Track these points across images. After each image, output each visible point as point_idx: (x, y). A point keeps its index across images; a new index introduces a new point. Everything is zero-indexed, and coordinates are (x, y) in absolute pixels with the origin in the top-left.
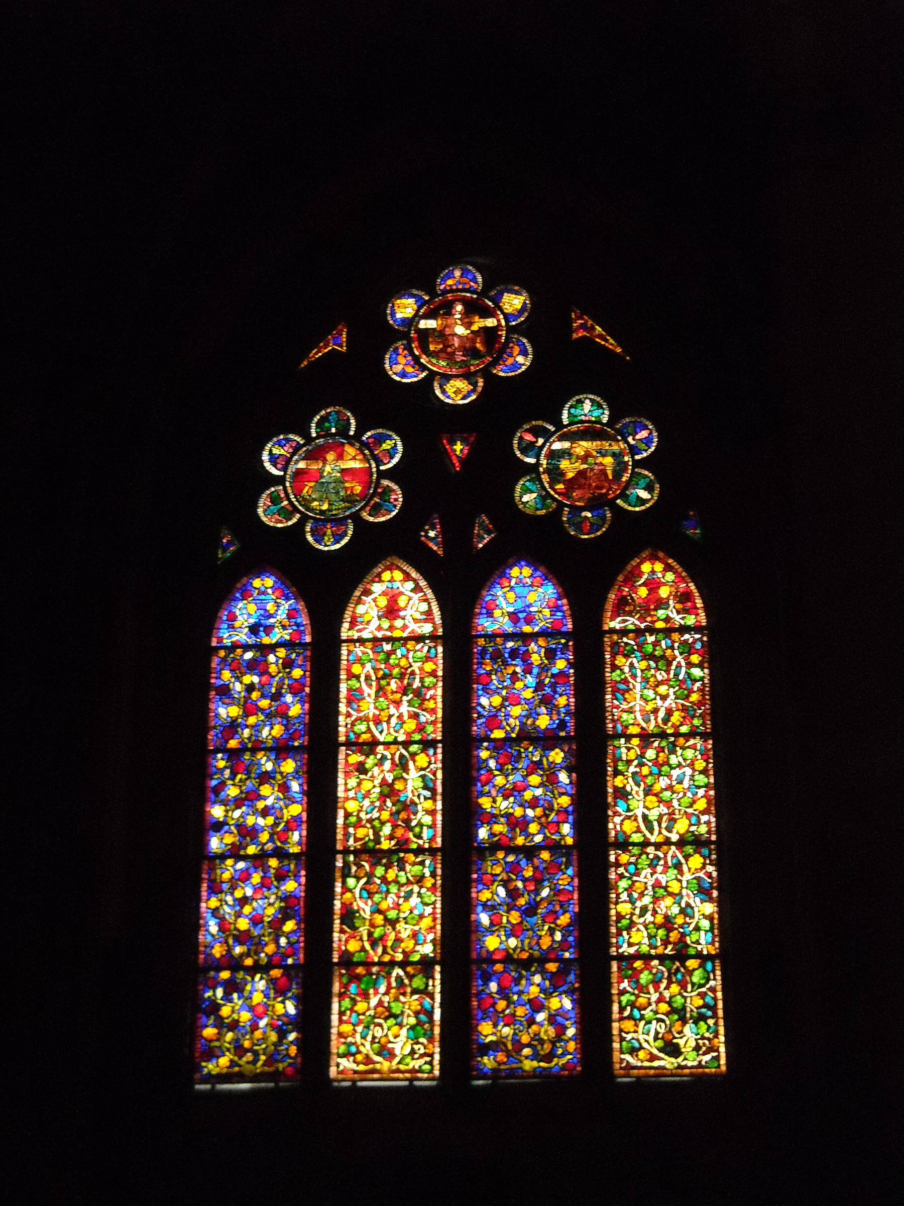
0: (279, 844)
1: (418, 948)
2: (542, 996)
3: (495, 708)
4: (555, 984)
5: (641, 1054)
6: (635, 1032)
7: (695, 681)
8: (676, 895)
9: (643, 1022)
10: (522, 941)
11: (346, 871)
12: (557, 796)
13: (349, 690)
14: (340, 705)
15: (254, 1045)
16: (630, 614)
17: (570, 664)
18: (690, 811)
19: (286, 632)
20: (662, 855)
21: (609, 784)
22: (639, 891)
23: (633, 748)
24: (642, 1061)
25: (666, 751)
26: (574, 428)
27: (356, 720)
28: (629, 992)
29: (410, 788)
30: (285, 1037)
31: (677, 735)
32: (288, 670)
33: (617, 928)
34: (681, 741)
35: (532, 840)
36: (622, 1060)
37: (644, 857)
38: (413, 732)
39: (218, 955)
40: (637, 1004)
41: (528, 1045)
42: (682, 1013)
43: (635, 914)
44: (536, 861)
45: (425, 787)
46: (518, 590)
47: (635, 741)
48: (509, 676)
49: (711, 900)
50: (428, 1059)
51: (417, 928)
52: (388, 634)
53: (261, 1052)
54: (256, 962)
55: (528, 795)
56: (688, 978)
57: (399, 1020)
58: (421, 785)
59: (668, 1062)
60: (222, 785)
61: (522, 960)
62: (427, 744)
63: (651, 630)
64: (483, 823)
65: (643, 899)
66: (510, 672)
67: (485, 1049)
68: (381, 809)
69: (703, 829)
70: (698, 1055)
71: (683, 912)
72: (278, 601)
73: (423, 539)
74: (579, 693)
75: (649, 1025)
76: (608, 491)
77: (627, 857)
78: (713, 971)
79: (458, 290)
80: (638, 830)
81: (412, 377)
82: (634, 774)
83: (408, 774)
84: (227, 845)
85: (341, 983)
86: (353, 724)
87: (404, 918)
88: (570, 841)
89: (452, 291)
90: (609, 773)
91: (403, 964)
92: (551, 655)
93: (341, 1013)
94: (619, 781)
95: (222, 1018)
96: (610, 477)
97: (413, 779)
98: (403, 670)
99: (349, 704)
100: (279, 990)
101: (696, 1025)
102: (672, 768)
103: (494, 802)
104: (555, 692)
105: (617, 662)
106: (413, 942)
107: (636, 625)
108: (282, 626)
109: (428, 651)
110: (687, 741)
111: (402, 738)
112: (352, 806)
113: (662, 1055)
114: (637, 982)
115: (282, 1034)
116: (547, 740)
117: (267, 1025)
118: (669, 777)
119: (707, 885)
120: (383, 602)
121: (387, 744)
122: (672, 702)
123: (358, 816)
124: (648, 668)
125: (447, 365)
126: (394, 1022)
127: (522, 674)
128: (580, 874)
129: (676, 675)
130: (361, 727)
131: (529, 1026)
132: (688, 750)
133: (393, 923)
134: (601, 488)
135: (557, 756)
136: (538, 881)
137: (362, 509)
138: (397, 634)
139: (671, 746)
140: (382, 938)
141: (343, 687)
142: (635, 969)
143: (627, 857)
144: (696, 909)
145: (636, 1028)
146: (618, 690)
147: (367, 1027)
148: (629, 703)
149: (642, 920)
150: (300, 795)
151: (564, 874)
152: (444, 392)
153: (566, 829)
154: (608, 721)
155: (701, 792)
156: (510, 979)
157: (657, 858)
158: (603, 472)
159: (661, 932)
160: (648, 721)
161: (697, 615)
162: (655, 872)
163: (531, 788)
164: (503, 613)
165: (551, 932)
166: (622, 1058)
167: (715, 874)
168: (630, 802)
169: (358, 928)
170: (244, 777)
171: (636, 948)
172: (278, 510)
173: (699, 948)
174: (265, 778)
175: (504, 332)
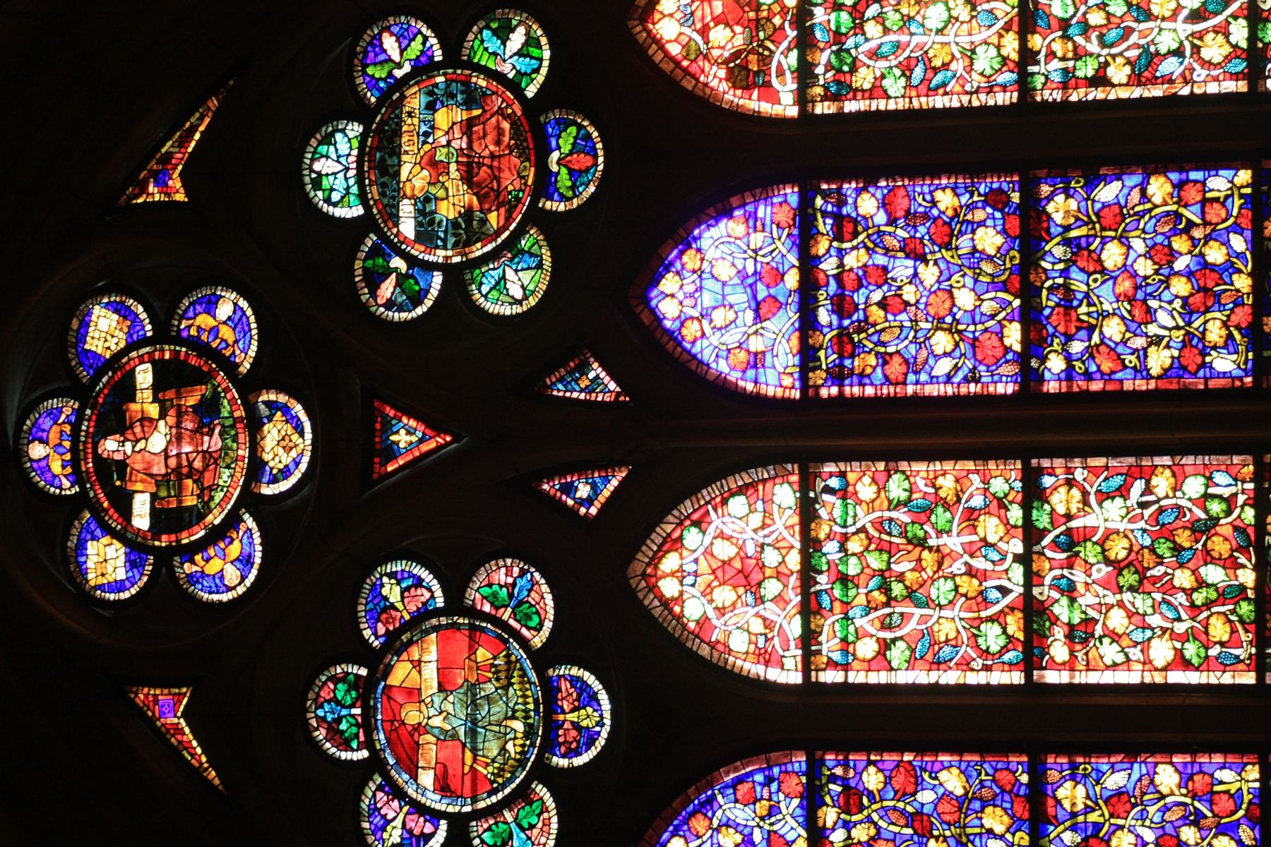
0: (1241, 813)
3: (957, 345)
12: (1148, 206)
13: (911, 663)
14: (942, 681)
16: (765, 60)
19: (782, 805)
21: (1124, 94)
23: (1049, 45)
26: (374, 192)
29: (1123, 526)
32: (865, 801)
35: (1240, 256)
45: (1123, 492)
46: (707, 300)
47: (1036, 41)
48: (890, 317)
52: (793, 581)
55: (1145, 267)
58: (1119, 501)
62: (1033, 494)
64: (1203, 365)
66: (882, 313)
68: (1170, 588)
72: (715, 823)
73: (593, 511)
74: (929, 169)
76: (506, 117)
79: (74, 450)
80: (1223, 30)
81: (251, 544)
82: (1103, 45)
83: (1095, 529)
86: (986, 653)
88: (1244, 176)
89: (75, 463)
92: (845, 227)
94: (1118, 73)
96: (480, 112)
97: (1110, 515)
98: (873, 547)
99: (937, 664)
103: (1156, 341)
104: (926, 216)
105: (867, 86)
107: (789, 49)
108: (770, 815)
111: (1017, 546)
112: (1162, 651)
120: (725, 595)
121: (1032, 578)
123: (1184, 638)
124: (880, 19)
125: (228, 467)
127: (885, 288)
130: (992, 637)
134: (500, 132)
135: (1060, 208)
137: (524, 643)
138: (794, 561)
141: (904, 678)
148: (953, 57)
150: (1136, 766)
152: (286, 473)
153: (1218, 184)
154: (991, 103)
163: (1129, 263)
164: (756, 332)
168: (1163, 51)
172: (523, 829)
175: (167, 347)
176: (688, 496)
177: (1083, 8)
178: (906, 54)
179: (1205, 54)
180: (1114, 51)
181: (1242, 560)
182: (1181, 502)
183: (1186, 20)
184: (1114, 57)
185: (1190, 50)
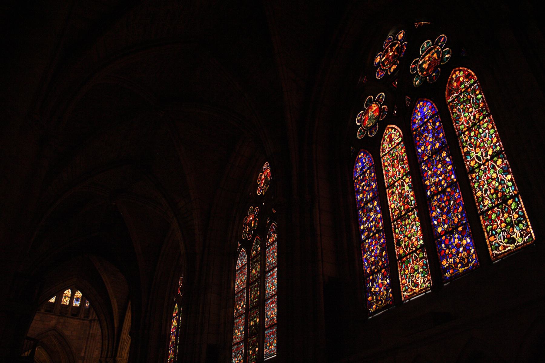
0: (377, 229)
1: (419, 243)
2: (459, 241)
4: (463, 236)
5: (500, 248)
7: (479, 100)
8: (496, 178)
9: (497, 235)
10: (449, 225)
11: (395, 228)
15: (381, 298)
16: (454, 94)
17: (440, 122)
18: (491, 145)
20: (486, 167)
22: (482, 185)
23: (467, 135)
24: (501, 251)
27: (389, 179)
28: (489, 225)
31: (479, 121)
33: (478, 203)
34: (481, 122)
35: (444, 187)
36: (493, 254)
37: (481, 171)
38: (403, 173)
39: (368, 272)
40: (493, 228)
42: (511, 224)
43: (483, 194)
44: (447, 193)
47: (467, 133)
49: (509, 173)
50: (428, 282)
53: (383, 299)
54: (378, 270)
56: (510, 208)
57: (418, 271)
59: (511, 247)
60: (362, 218)
61: (450, 231)
63: (461, 94)
67: (446, 270)
69: (498, 148)
70: (523, 239)
71: (500, 184)
75: (500, 235)
78: (519, 200)
82: (469, 144)
83: (404, 187)
87: (413, 235)
90: (461, 149)
91: (416, 250)
93: (402, 276)
95: (372, 292)
99: (386, 174)
100: (384, 276)
101: (518, 226)
102: (481, 134)
106: (417, 242)
109: (402, 146)
110: (483, 122)
112: (392, 206)
113: (508, 245)
114: (491, 220)
115: (387, 290)
116: (438, 152)
118: (481, 137)
122: (474, 112)
124: (464, 106)
126: (416, 273)
128: (461, 190)
129: (473, 102)
131: (458, 255)
132: (485, 124)
133: (410, 238)
136: (449, 200)
138: (394, 146)
139: (478, 126)
140: (408, 245)
142: (489, 215)
143: (475, 174)
144: (505, 180)
145: (495, 238)
146: (457, 120)
147: (409, 278)
149: (486, 195)
151: (456, 193)
153: (453, 176)
155: (493, 136)
157: (485, 168)
158: (435, 58)
159: (494, 196)
162: (486, 175)
165: (457, 216)
167: (508, 162)
169: (401, 245)
170: (366, 213)
171: (487, 207)
173: (511, 194)
174: (371, 210)
177: (473, 137)
178: (460, 114)
179: (471, 162)
181: (405, 211)
182: (410, 198)
183: (476, 156)
184: (468, 147)
185: (472, 159)
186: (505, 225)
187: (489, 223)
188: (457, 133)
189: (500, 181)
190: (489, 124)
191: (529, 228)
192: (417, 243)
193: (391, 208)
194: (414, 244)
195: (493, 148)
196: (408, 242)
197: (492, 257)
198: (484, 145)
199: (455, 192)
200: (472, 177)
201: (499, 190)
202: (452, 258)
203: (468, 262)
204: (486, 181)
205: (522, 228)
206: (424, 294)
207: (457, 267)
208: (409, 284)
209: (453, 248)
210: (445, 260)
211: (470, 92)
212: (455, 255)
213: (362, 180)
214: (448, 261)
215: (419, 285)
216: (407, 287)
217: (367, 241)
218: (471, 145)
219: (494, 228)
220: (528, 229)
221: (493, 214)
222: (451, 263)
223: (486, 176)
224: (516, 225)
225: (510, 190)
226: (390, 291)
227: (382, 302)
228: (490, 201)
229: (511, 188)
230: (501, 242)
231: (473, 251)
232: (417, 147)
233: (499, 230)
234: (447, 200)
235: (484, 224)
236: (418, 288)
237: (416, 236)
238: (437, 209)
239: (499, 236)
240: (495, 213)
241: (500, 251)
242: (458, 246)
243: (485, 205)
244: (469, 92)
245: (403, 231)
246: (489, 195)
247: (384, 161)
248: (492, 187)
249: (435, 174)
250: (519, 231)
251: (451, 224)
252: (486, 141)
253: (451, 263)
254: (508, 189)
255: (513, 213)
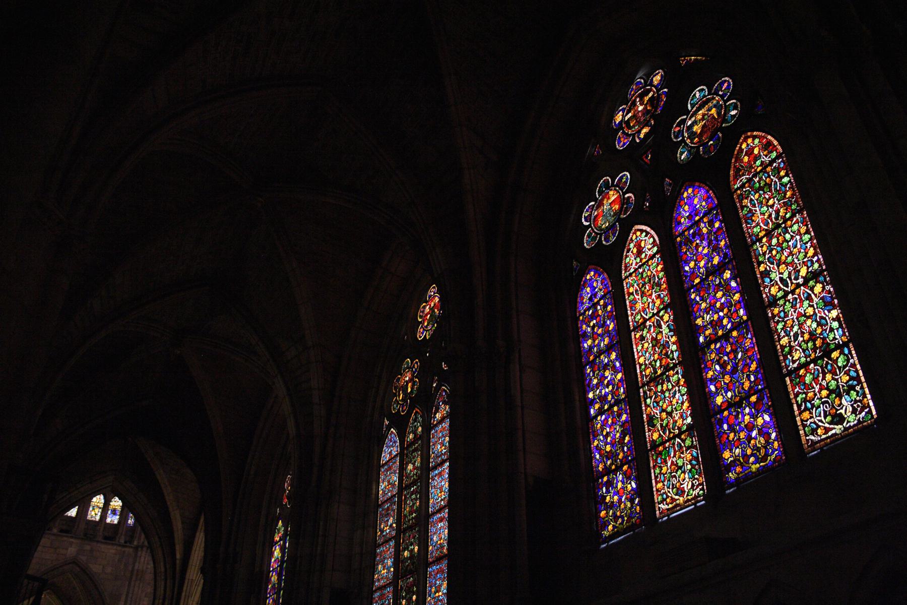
1: (685, 422)
2: (752, 420)
4: (758, 409)
5: (819, 431)
6: (811, 417)
7: (785, 186)
8: (812, 315)
9: (814, 409)
15: (621, 513)
16: (743, 175)
17: (721, 222)
18: (805, 260)
20: (797, 296)
22: (790, 326)
23: (764, 244)
24: (821, 436)
25: (783, 235)
27: (635, 315)
28: (800, 393)
30: (634, 503)
33: (783, 355)
34: (789, 223)
35: (727, 329)
36: (808, 441)
37: (787, 303)
39: (601, 470)
40: (808, 398)
41: (752, 455)
42: (838, 390)
43: (792, 341)
44: (731, 340)
47: (764, 240)
49: (834, 307)
50: (700, 487)
51: (682, 411)
53: (625, 515)
54: (616, 466)
57: (683, 469)
59: (838, 429)
60: (591, 380)
61: (737, 402)
63: (755, 176)
65: (794, 329)
67: (730, 467)
69: (816, 266)
70: (856, 416)
71: (819, 324)
75: (819, 409)
77: (778, 309)
82: (768, 258)
83: (662, 329)
84: (597, 410)
85: (653, 460)
87: (675, 408)
90: (755, 267)
91: (681, 433)
93: (656, 477)
100: (628, 477)
101: (849, 395)
102: (788, 242)
106: (681, 420)
109: (658, 260)
110: (792, 221)
112: (642, 360)
113: (832, 426)
115: (632, 501)
116: (718, 270)
117: (625, 499)
118: (788, 247)
119: (829, 299)
124: (760, 196)
126: (681, 471)
128: (755, 335)
129: (775, 189)
131: (749, 442)
132: (794, 226)
133: (670, 414)
136: (734, 351)
138: (644, 260)
140: (667, 425)
142: (801, 376)
143: (778, 309)
144: (827, 318)
145: (811, 415)
147: (669, 480)
153: (741, 312)
155: (809, 245)
156: (733, 417)
158: (714, 117)
159: (810, 344)
160: (767, 224)
161: (777, 149)
162: (796, 309)
165: (748, 377)
166: (807, 438)
167: (832, 289)
168: (771, 276)
169: (656, 425)
170: (598, 372)
171: (797, 363)
173: (836, 341)
174: (605, 367)
176: (651, 228)
177: (775, 247)
178: (753, 209)
179: (772, 289)
180: (768, 263)
182: (671, 346)
184: (766, 264)
185: (773, 283)
186: (828, 392)
187: (802, 390)
188: (749, 240)
189: (818, 320)
190: (801, 225)
191: (866, 397)
192: (681, 423)
193: (639, 363)
194: (677, 424)
195: (807, 266)
196: (666, 419)
197: (806, 445)
198: (793, 260)
199: (745, 337)
200: (773, 314)
201: (818, 335)
202: (740, 447)
203: (767, 455)
204: (796, 320)
205: (855, 399)
206: (693, 507)
207: (747, 462)
208: (668, 490)
209: (741, 430)
210: (728, 450)
211: (770, 173)
212: (744, 443)
213: (592, 317)
214: (733, 452)
215: (685, 492)
216: (665, 496)
217: (599, 418)
218: (771, 260)
219: (810, 398)
220: (865, 399)
221: (808, 375)
222: (739, 455)
223: (797, 312)
224: (845, 394)
225: (835, 334)
226: (636, 502)
227: (623, 520)
228: (802, 354)
229: (838, 331)
230: (821, 421)
231: (773, 435)
232: (683, 263)
233: (817, 402)
234: (732, 351)
235: (793, 390)
236: (683, 497)
237: (680, 410)
238: (715, 365)
239: (817, 411)
240: (811, 373)
241: (818, 435)
242: (750, 427)
243: (794, 359)
244: (768, 173)
245: (659, 402)
246: (801, 343)
247: (628, 286)
248: (806, 331)
249: (711, 308)
250: (850, 404)
251: (738, 390)
252: (796, 254)
253: (737, 456)
254: (833, 333)
255: (840, 374)
